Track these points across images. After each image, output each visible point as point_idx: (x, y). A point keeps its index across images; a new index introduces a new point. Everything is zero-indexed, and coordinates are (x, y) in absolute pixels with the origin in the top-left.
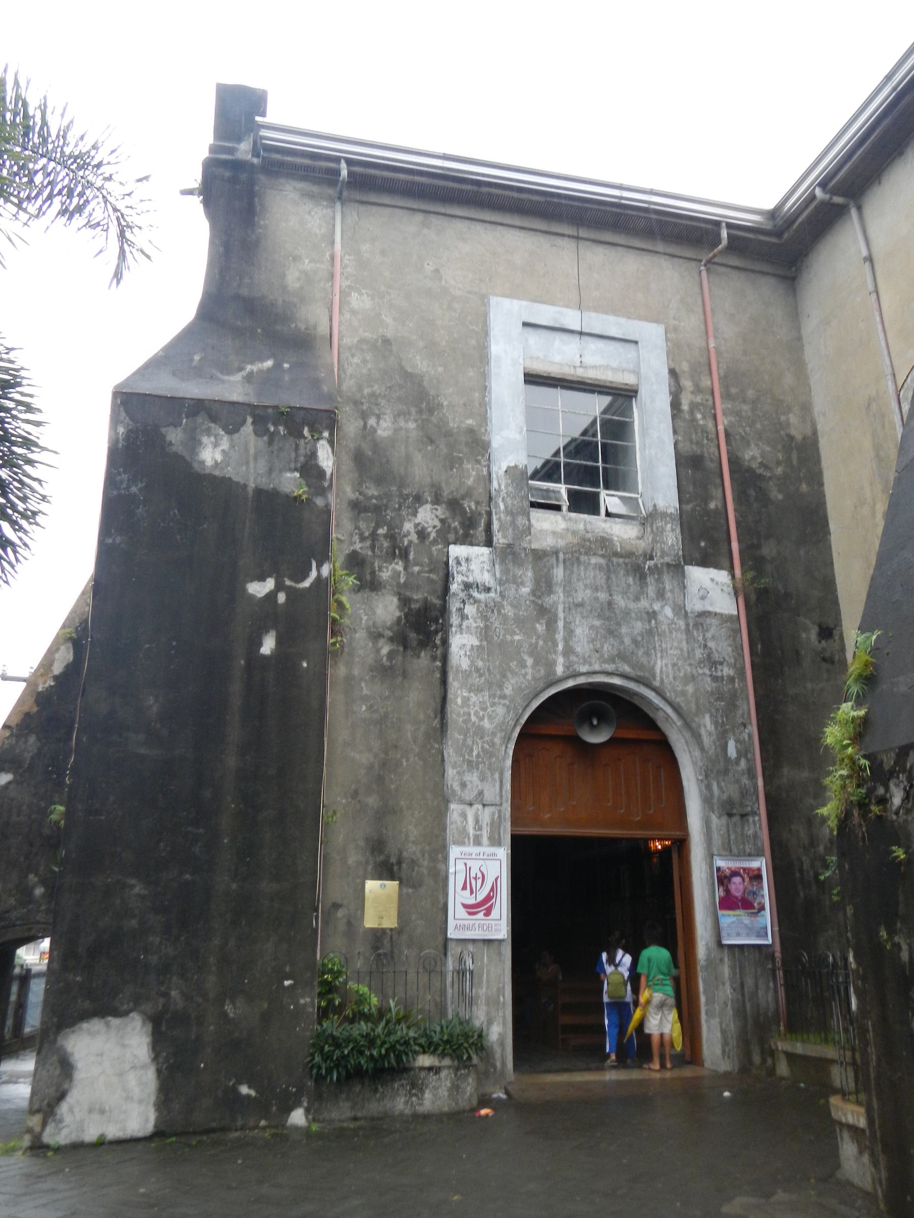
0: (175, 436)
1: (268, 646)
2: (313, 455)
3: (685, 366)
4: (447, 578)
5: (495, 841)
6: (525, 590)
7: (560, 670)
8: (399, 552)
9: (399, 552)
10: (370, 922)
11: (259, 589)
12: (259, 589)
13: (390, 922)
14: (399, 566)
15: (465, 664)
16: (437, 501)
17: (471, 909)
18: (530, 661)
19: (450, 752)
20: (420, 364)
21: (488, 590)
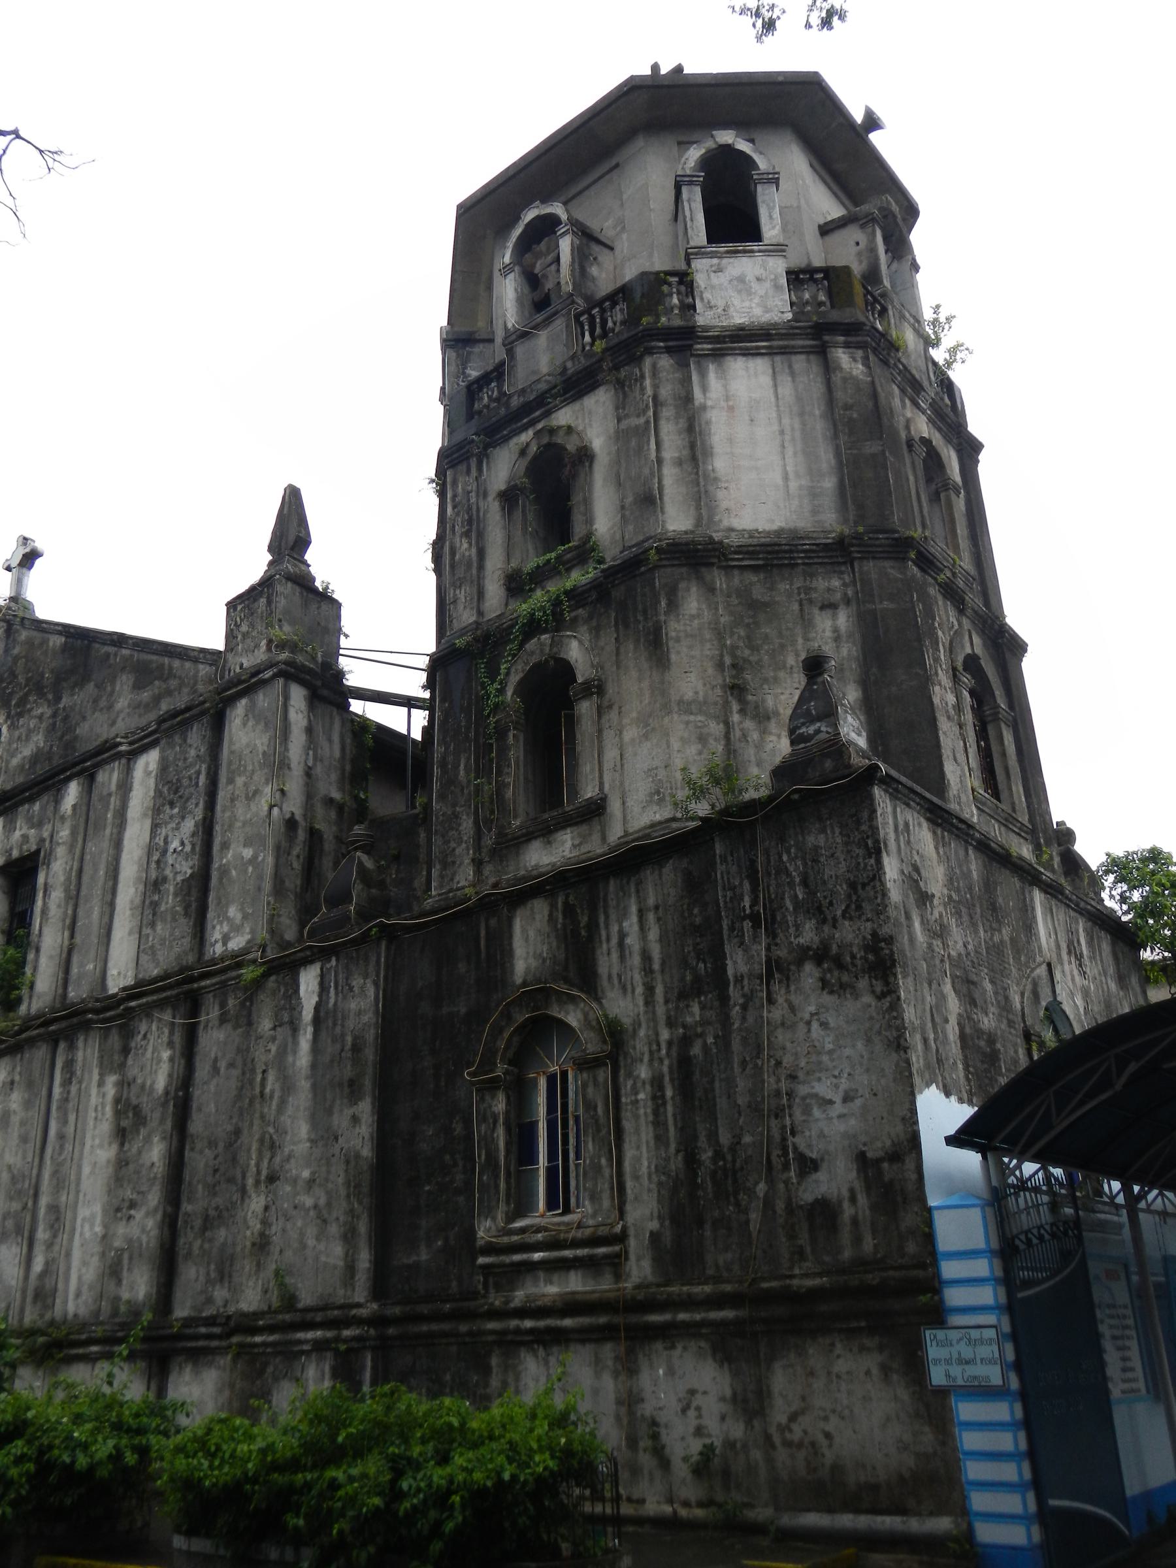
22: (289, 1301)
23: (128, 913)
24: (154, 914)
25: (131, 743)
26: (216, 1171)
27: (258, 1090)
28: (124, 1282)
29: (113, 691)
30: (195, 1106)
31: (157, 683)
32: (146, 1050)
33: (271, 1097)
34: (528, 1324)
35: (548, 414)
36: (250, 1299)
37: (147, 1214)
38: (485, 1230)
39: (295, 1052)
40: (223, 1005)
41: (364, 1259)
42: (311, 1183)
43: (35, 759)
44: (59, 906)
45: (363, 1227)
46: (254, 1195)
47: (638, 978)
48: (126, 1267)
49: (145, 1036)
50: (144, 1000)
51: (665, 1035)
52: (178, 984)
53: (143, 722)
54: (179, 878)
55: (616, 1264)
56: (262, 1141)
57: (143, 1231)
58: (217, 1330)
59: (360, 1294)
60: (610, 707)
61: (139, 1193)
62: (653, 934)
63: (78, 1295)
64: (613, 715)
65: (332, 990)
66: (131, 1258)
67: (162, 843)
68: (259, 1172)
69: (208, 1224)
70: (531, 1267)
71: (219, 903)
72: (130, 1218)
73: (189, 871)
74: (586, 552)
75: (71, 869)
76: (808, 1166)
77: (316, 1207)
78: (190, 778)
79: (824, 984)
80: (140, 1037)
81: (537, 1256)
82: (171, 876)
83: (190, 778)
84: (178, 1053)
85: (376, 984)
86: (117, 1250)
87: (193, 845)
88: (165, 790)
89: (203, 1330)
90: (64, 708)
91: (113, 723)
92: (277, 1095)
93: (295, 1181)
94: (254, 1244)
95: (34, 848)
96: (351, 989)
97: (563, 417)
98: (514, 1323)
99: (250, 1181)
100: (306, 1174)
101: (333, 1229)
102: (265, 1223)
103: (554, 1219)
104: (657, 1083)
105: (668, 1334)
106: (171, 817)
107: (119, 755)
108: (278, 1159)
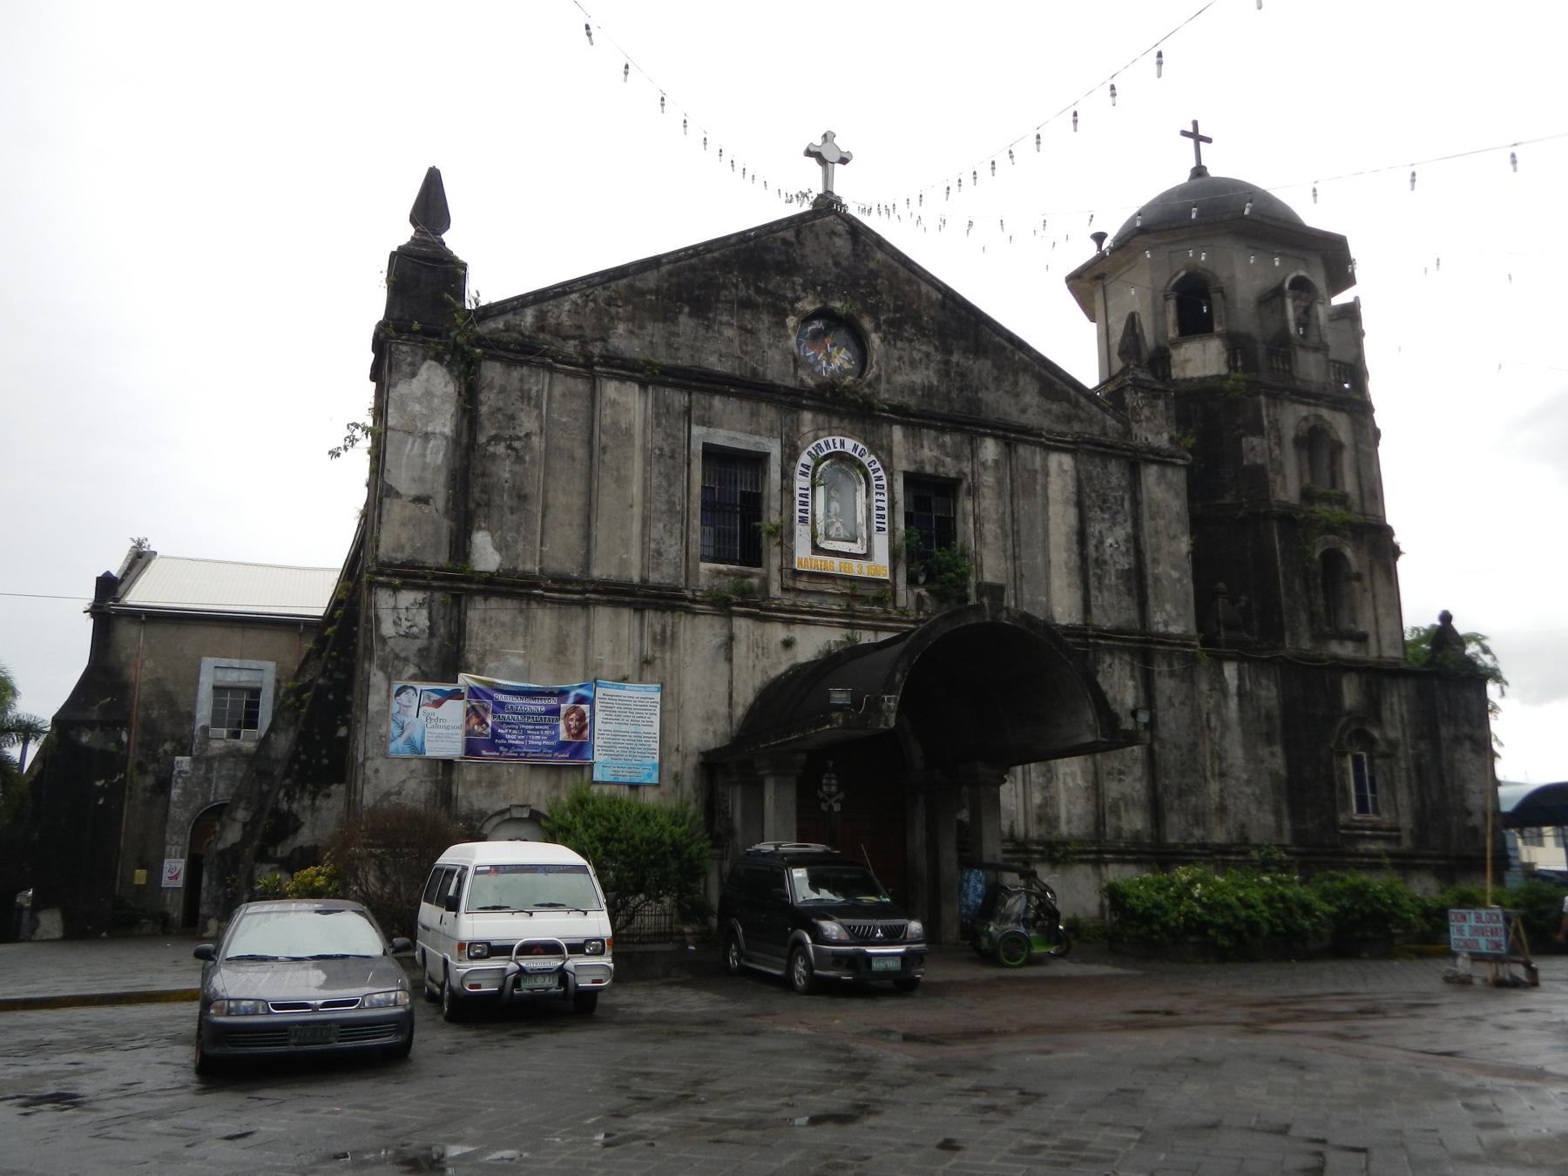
0: (72, 733)
1: (101, 802)
2: (120, 737)
3: (284, 677)
4: (173, 769)
5: (181, 857)
6: (201, 772)
7: (211, 799)
8: (156, 760)
9: (156, 760)
10: (137, 882)
11: (99, 783)
12: (99, 783)
13: (143, 882)
14: (156, 765)
15: (176, 799)
16: (172, 740)
17: (170, 878)
18: (200, 797)
19: (168, 829)
20: (171, 687)
21: (187, 773)
22: (1245, 840)
23: (1064, 570)
24: (1100, 583)
25: (1048, 439)
26: (1183, 764)
27: (1205, 724)
28: (1123, 819)
29: (1016, 384)
30: (1159, 721)
31: (1065, 404)
32: (1112, 675)
33: (1215, 729)
34: (1366, 860)
35: (1316, 405)
36: (1219, 836)
37: (1135, 780)
38: (1342, 818)
39: (1227, 708)
40: (1170, 665)
41: (1287, 824)
42: (1248, 782)
43: (929, 392)
44: (996, 538)
45: (1285, 808)
46: (1211, 781)
47: (1398, 724)
48: (1122, 810)
49: (1110, 666)
50: (1108, 642)
51: (1411, 752)
52: (1139, 641)
53: (1059, 428)
54: (1119, 567)
55: (1398, 840)
56: (1212, 753)
57: (1133, 789)
58: (1207, 852)
59: (1287, 840)
60: (1365, 590)
61: (1125, 766)
62: (1404, 708)
63: (1069, 822)
64: (1369, 596)
65: (1247, 682)
66: (1126, 805)
67: (1097, 533)
68: (1213, 770)
69: (1182, 793)
70: (1363, 837)
71: (1156, 598)
72: (1120, 780)
73: (1127, 567)
74: (1343, 500)
75: (1004, 513)
76: (1470, 814)
77: (1254, 794)
78: (1115, 497)
79: (1473, 751)
80: (1105, 666)
81: (1368, 832)
82: (1110, 562)
83: (1115, 497)
84: (1140, 684)
85: (1276, 686)
86: (1113, 798)
87: (1128, 550)
88: (1093, 495)
89: (1197, 851)
90: (958, 364)
91: (1023, 411)
92: (1219, 729)
93: (1237, 779)
94: (1217, 808)
95: (953, 475)
96: (1260, 684)
97: (1326, 413)
98: (1359, 860)
99: (1208, 774)
100: (1245, 776)
101: (1266, 807)
102: (1221, 797)
103: (1374, 818)
104: (1408, 770)
105: (1418, 868)
106: (1103, 519)
107: (1041, 445)
108: (1224, 765)
